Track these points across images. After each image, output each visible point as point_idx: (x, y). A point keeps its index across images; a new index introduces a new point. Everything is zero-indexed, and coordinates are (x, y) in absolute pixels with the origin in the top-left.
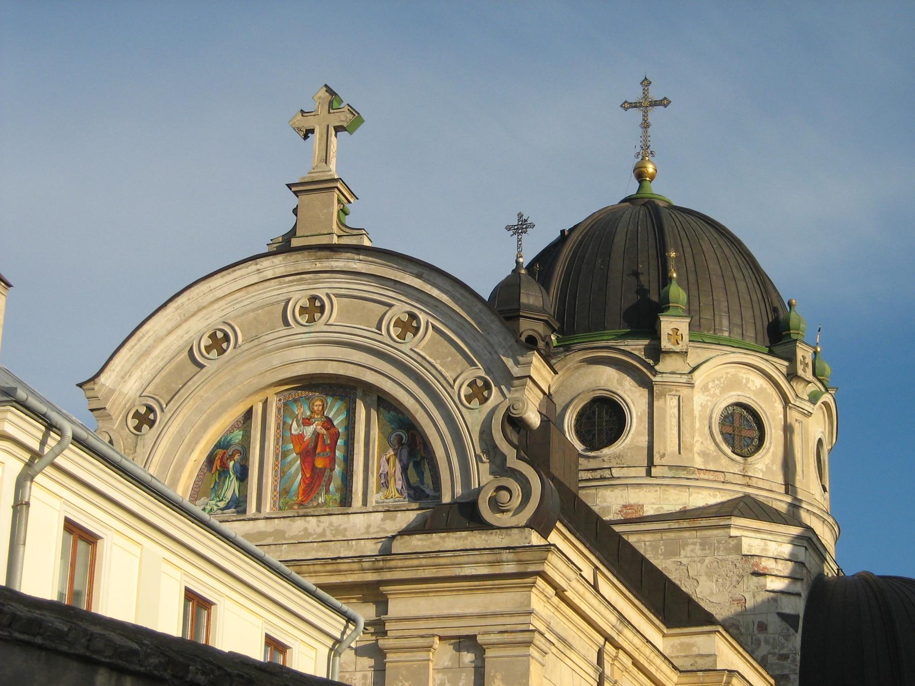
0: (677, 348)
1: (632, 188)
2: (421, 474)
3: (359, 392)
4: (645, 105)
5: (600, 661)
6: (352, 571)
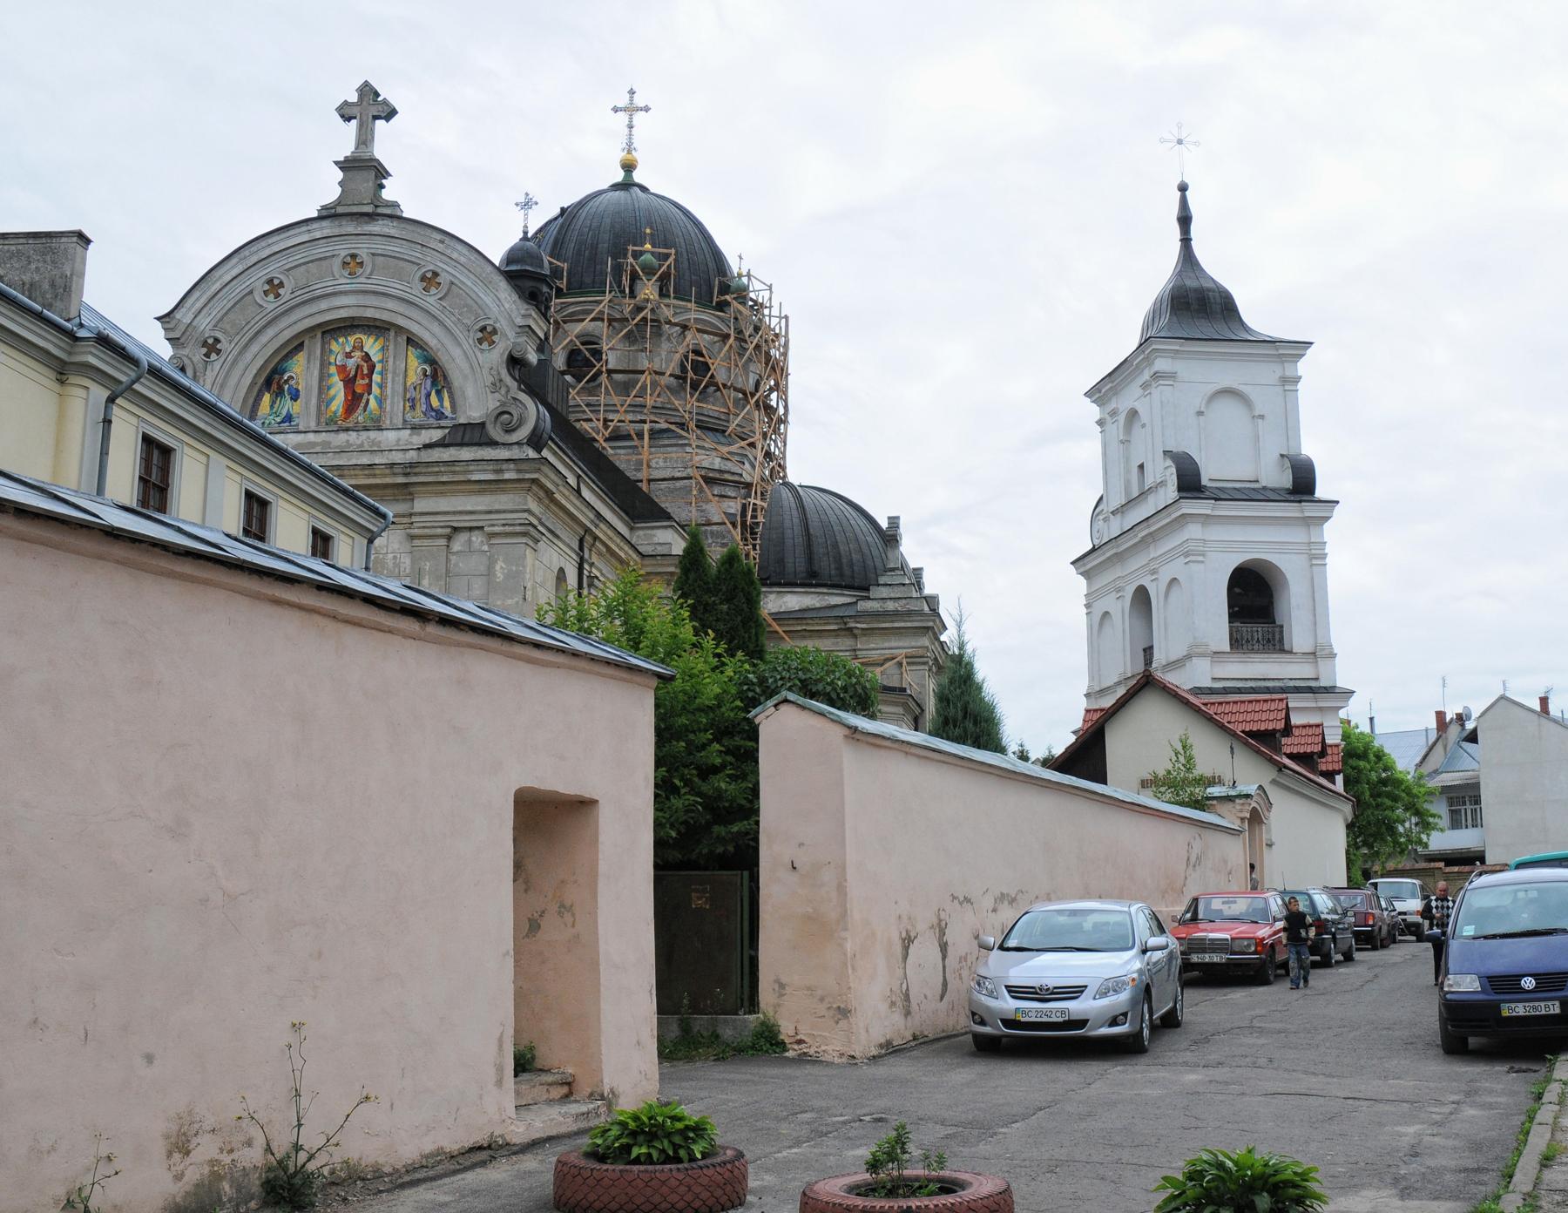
1: (619, 176)
2: (441, 400)
3: (392, 333)
4: (631, 109)
5: (581, 548)
6: (385, 476)
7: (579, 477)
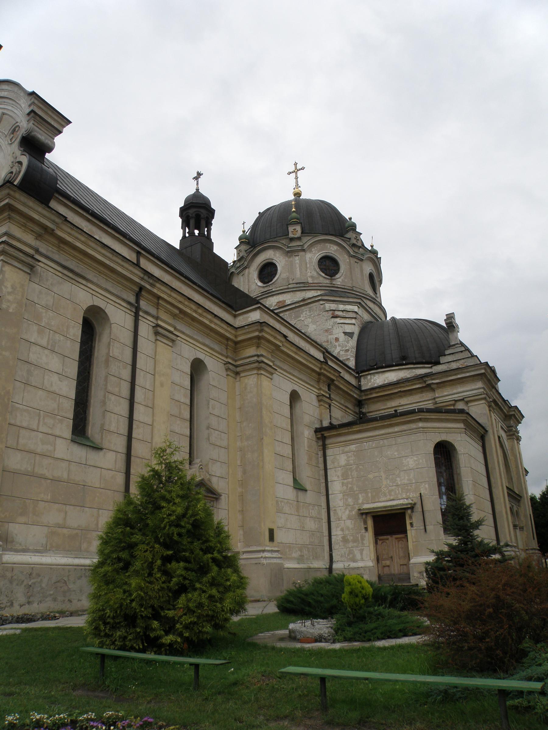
0: (296, 236)
4: (296, 171)
5: (137, 301)
7: (138, 253)
